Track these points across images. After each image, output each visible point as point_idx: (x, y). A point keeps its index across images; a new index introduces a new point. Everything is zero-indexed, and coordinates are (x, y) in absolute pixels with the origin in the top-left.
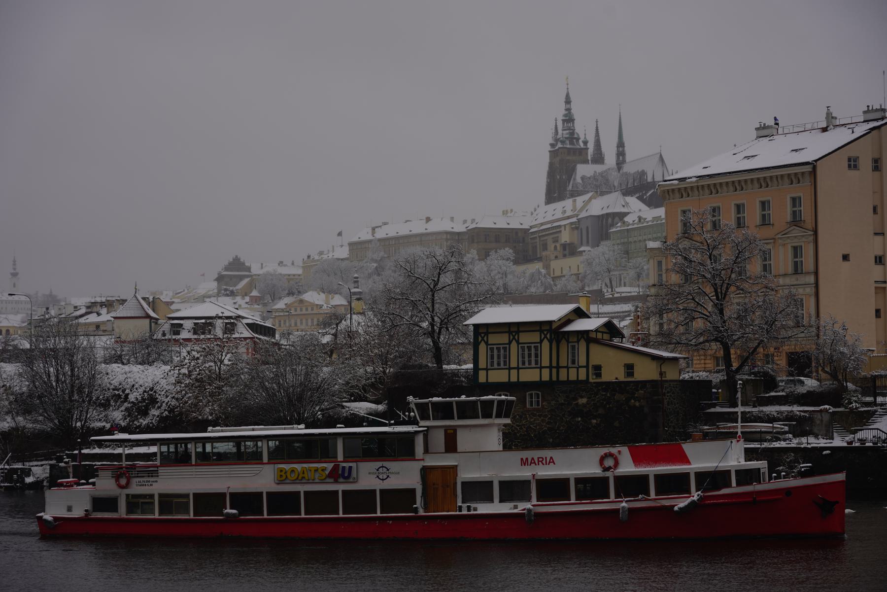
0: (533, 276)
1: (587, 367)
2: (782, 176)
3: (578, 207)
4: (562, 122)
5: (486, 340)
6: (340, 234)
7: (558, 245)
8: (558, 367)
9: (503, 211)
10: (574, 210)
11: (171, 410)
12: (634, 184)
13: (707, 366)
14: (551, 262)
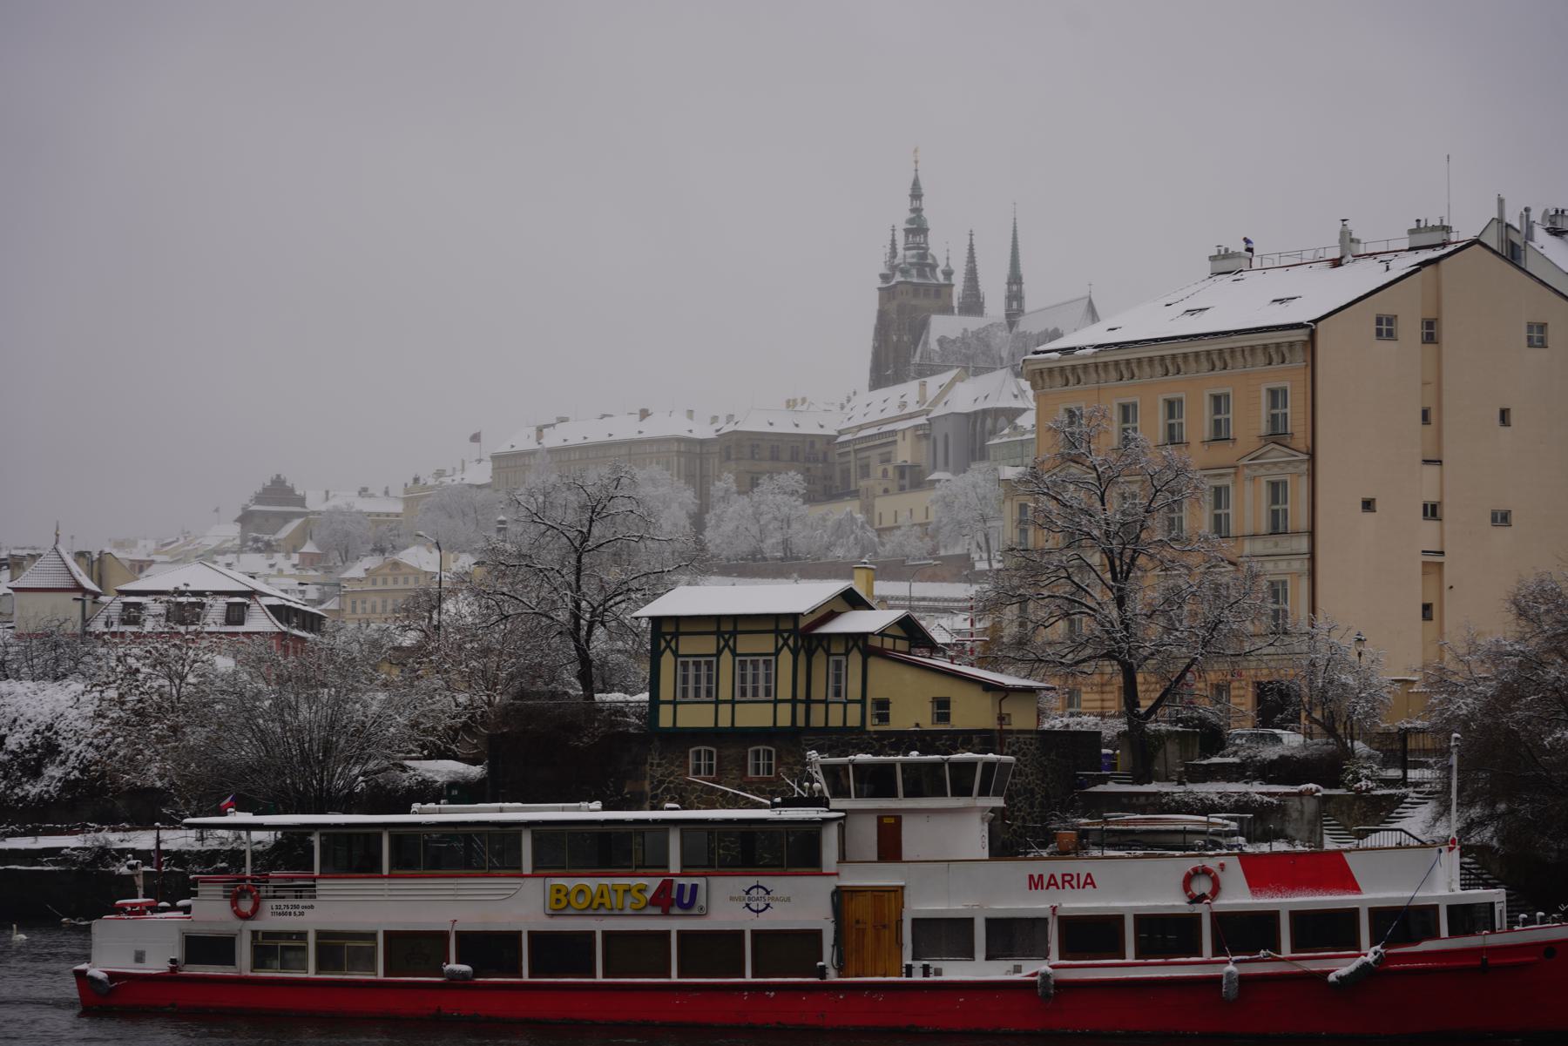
0: (840, 524)
1: (863, 701)
2: (1252, 348)
3: (930, 398)
4: (904, 233)
5: (674, 648)
6: (476, 438)
7: (890, 468)
8: (808, 701)
9: (788, 402)
10: (921, 402)
13: (1107, 704)
14: (877, 499)
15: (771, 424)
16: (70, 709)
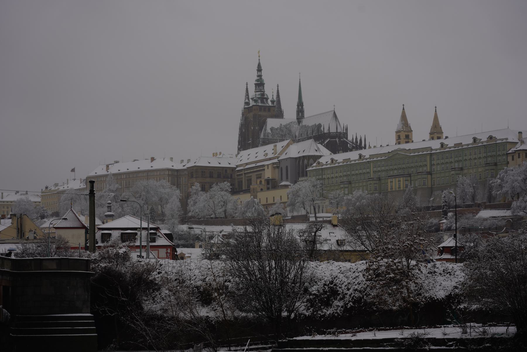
3: (278, 152)
4: (254, 85)
6: (73, 170)
9: (214, 154)
10: (275, 153)
11: (357, 301)
15: (209, 163)
16: (339, 274)
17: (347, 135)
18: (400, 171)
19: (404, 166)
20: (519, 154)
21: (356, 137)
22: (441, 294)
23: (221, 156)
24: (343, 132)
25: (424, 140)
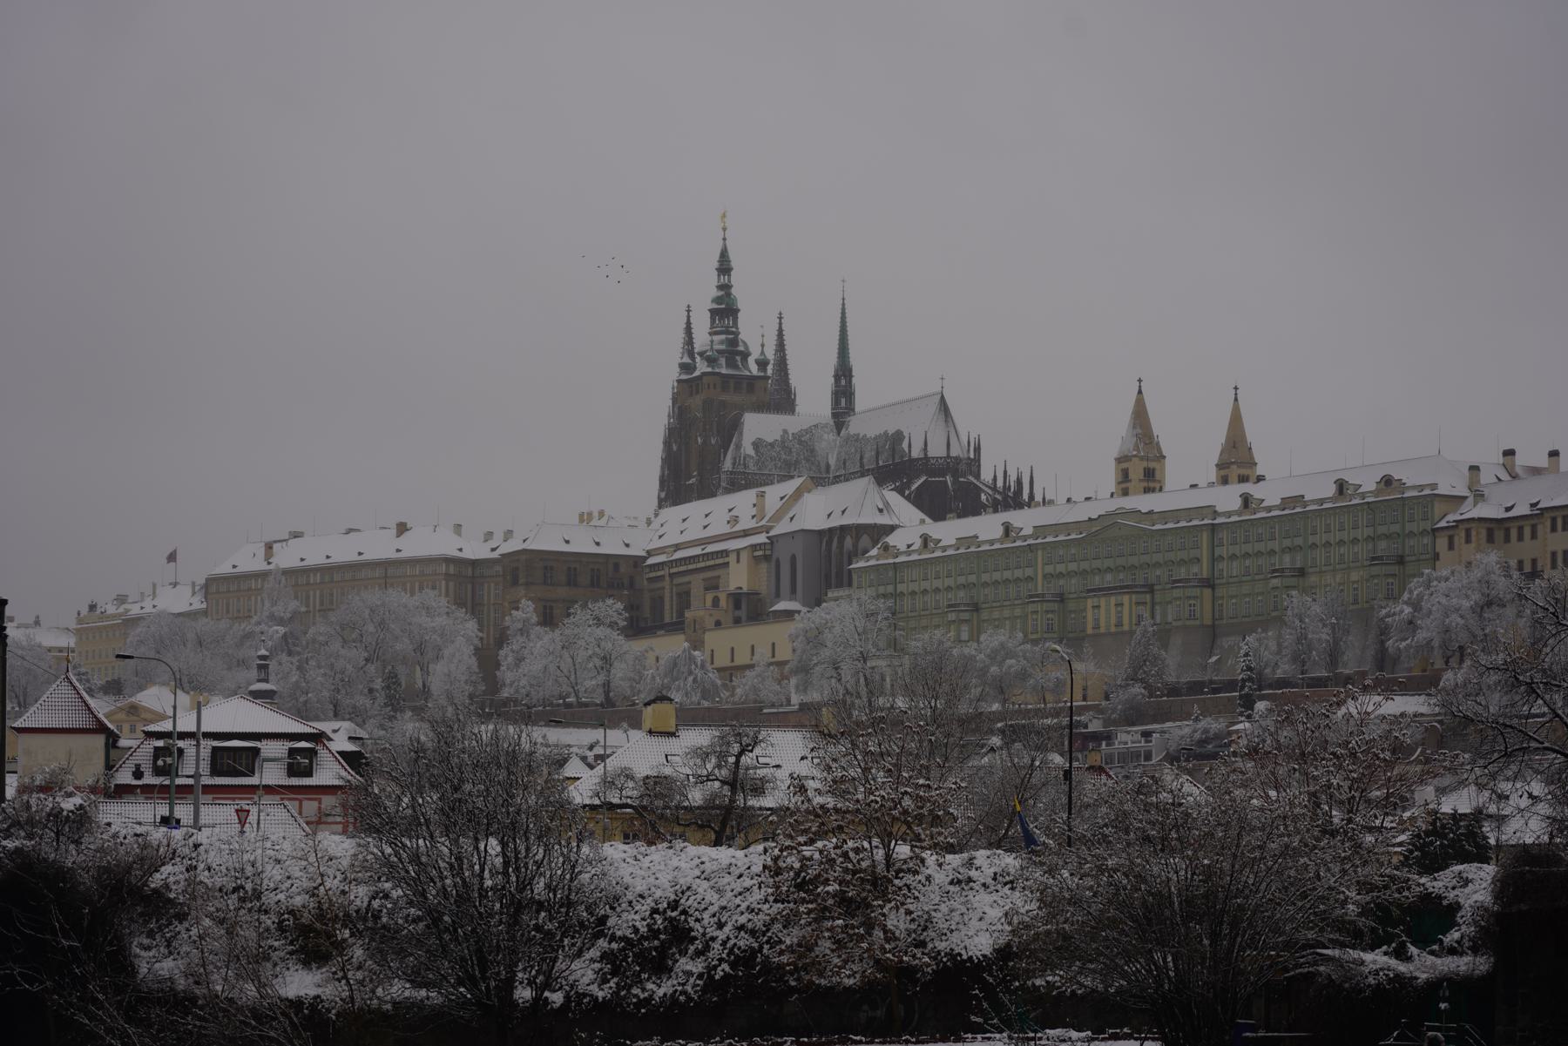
0: (675, 665)
3: (770, 510)
4: (709, 314)
6: (172, 557)
7: (723, 597)
9: (582, 515)
11: (744, 959)
12: (878, 463)
14: (707, 633)
15: (567, 542)
16: (697, 880)
17: (979, 466)
18: (1121, 576)
19: (1134, 560)
20: (1468, 532)
21: (1005, 472)
22: (979, 943)
23: (603, 522)
24: (966, 456)
25: (1194, 486)
